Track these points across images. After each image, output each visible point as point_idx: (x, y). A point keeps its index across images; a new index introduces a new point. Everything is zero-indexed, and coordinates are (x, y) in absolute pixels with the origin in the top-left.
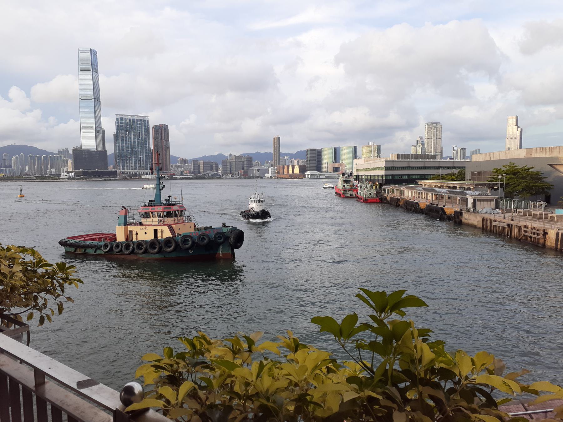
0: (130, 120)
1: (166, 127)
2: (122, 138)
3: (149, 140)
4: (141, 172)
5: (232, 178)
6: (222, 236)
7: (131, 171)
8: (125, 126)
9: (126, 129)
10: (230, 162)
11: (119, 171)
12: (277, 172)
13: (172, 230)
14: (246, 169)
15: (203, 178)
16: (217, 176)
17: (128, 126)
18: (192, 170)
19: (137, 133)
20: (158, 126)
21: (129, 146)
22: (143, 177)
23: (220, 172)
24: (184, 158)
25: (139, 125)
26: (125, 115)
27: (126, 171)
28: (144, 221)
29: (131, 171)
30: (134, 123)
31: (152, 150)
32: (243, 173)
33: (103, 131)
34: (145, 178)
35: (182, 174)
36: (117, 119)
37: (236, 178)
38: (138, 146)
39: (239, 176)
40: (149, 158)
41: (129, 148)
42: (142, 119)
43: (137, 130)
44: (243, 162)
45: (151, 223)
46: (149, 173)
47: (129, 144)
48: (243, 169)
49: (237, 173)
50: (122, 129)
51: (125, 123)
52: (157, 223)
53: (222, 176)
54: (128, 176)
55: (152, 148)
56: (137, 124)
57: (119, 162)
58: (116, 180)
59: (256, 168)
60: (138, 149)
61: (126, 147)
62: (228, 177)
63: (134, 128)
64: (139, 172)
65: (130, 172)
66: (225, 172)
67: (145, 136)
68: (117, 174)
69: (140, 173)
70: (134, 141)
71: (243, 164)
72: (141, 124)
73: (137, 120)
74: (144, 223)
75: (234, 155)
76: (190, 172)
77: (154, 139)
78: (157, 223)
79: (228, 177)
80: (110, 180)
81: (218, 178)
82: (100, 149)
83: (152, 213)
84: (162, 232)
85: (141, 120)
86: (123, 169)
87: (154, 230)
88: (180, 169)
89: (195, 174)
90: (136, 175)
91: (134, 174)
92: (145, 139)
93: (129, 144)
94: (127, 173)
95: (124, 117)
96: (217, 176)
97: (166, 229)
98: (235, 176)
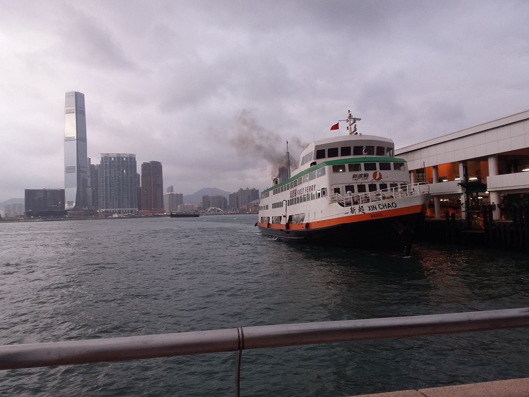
2: (106, 177)
8: (110, 165)
9: (110, 168)
30: (119, 162)
36: (102, 158)
50: (106, 168)
51: (110, 162)
57: (103, 201)
64: (123, 211)
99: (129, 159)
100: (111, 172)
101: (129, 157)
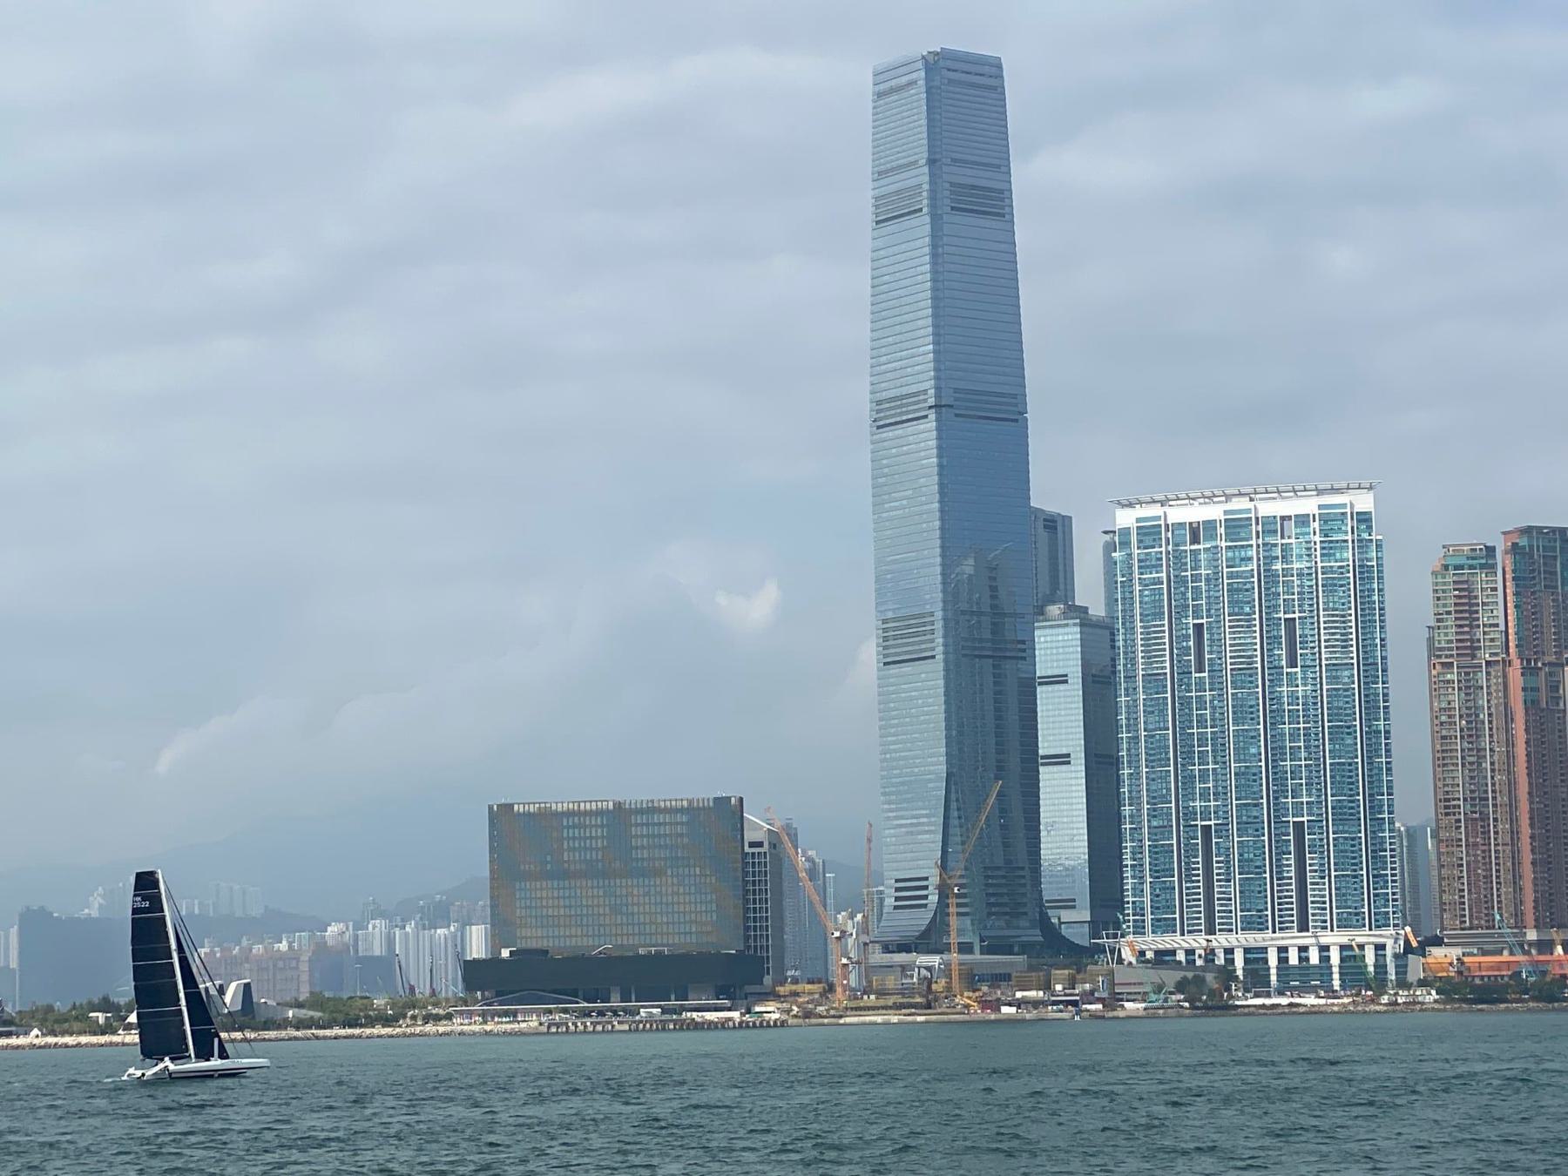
17: (1196, 578)
27: (1176, 942)
47: (1202, 722)
69: (1293, 959)
101: (1317, 512)
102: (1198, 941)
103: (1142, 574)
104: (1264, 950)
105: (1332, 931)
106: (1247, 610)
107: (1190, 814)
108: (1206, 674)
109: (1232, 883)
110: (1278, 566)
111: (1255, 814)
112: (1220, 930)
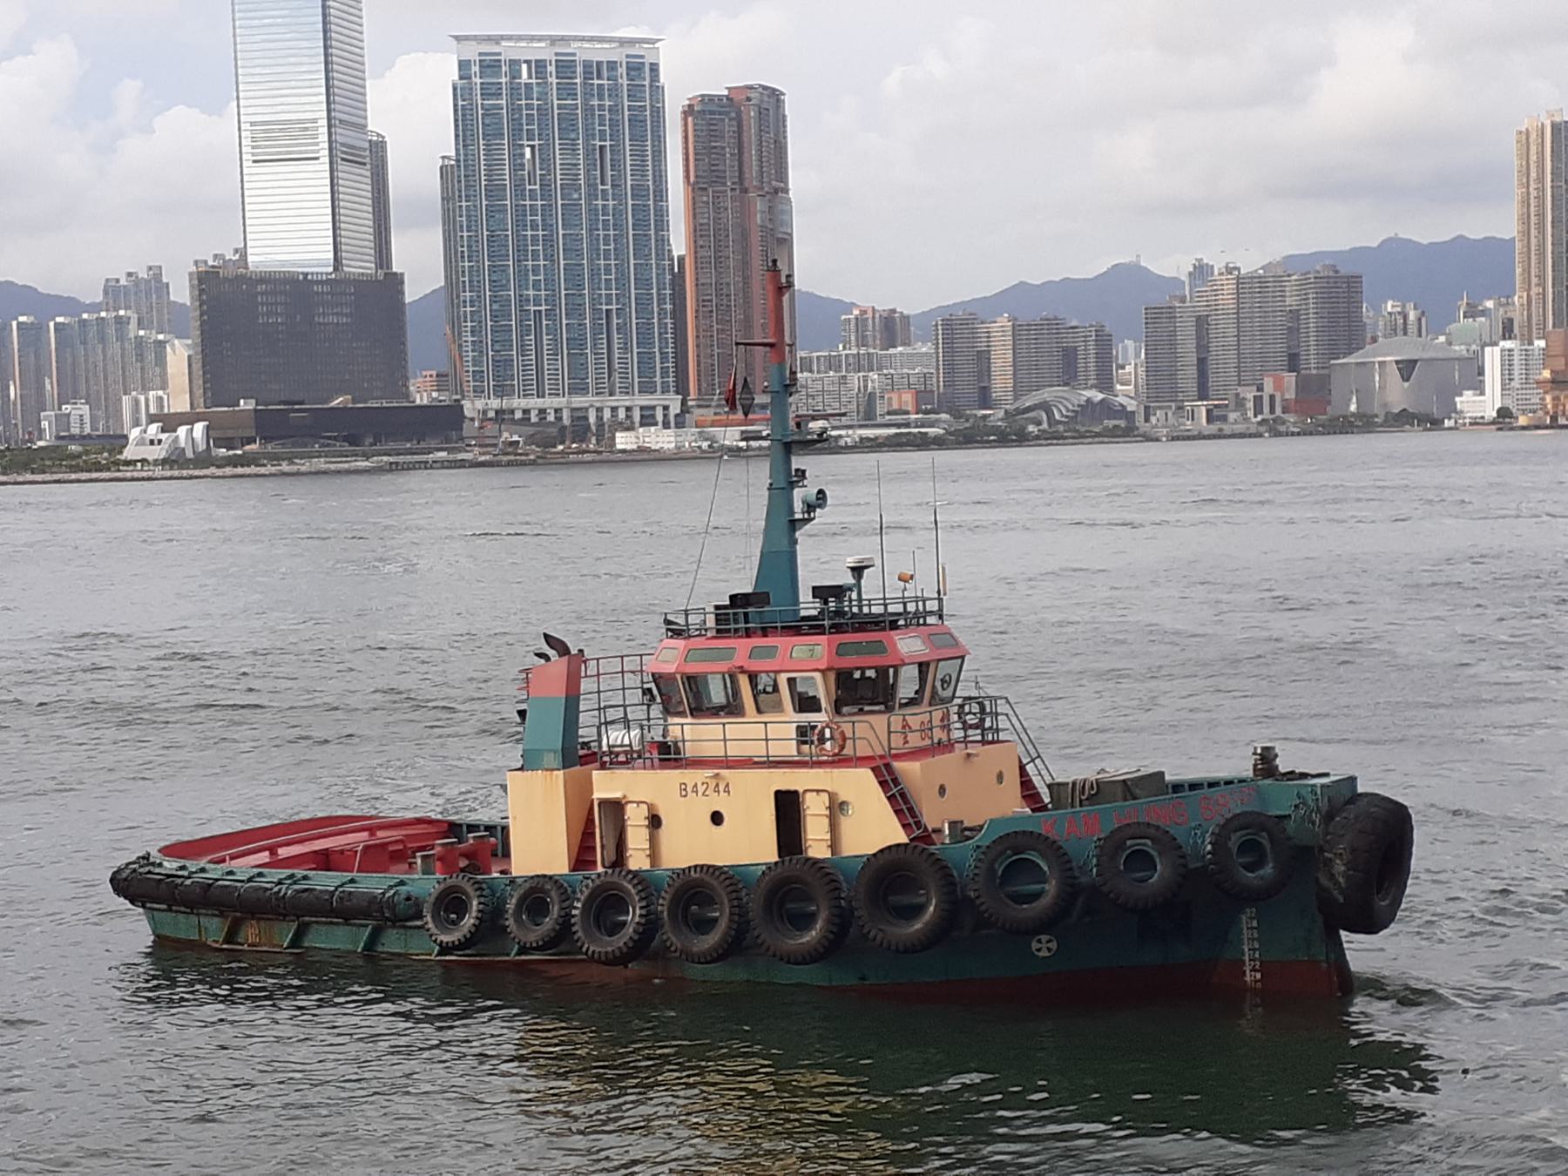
0: (540, 66)
1: (769, 104)
2: (494, 191)
3: (661, 193)
4: (614, 409)
5: (1213, 428)
6: (1264, 839)
7: (549, 402)
8: (514, 109)
9: (516, 132)
10: (1201, 322)
11: (480, 404)
12: (1547, 374)
13: (902, 803)
14: (1311, 362)
15: (1012, 436)
16: (1111, 423)
17: (529, 107)
18: (938, 384)
19: (589, 152)
20: (720, 98)
21: (535, 239)
22: (623, 440)
23: (1126, 394)
24: (883, 306)
25: (601, 98)
26: (510, 38)
27: (518, 403)
28: (694, 734)
29: (549, 402)
30: (566, 91)
31: (681, 259)
32: (1291, 395)
33: (378, 150)
34: (641, 450)
35: (868, 416)
36: (464, 65)
37: (1240, 428)
38: (594, 240)
39: (1266, 414)
40: (662, 311)
41: (535, 256)
42: (618, 55)
43: (589, 136)
44: (1295, 315)
45: (757, 750)
46: (660, 418)
48: (1293, 363)
49: (1249, 394)
50: (493, 134)
51: (514, 89)
52: (790, 749)
53: (1140, 418)
54: (530, 440)
55: (679, 243)
56: (588, 95)
58: (462, 464)
59: (1385, 354)
60: (591, 260)
61: (521, 249)
62: (1189, 424)
63: (567, 122)
64: (600, 410)
65: (542, 411)
66: (1160, 386)
67: (639, 168)
68: (469, 429)
69: (607, 414)
70: (571, 209)
71: (1293, 331)
72: (614, 91)
73: (587, 65)
74: (689, 751)
75: (1229, 270)
76: (922, 396)
77: (698, 187)
78: (790, 749)
79: (1189, 424)
80: (426, 465)
81: (1114, 435)
82: (361, 265)
83: (753, 678)
84: (837, 808)
85: (612, 66)
86: (502, 391)
87: (778, 794)
88: (855, 379)
89: (957, 414)
90: (579, 428)
91: (566, 421)
92: (639, 193)
93: (534, 227)
94: (526, 420)
95: (508, 51)
96: (1111, 423)
97: (860, 786)
98: (1232, 416)
99: (622, 70)
100: (523, 155)
102: (534, 403)
103: (483, 100)
104: (587, 409)
105: (633, 395)
106: (573, 136)
107: (523, 300)
108: (537, 187)
109: (560, 357)
110: (595, 102)
111: (579, 302)
112: (550, 394)
